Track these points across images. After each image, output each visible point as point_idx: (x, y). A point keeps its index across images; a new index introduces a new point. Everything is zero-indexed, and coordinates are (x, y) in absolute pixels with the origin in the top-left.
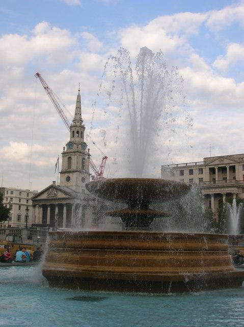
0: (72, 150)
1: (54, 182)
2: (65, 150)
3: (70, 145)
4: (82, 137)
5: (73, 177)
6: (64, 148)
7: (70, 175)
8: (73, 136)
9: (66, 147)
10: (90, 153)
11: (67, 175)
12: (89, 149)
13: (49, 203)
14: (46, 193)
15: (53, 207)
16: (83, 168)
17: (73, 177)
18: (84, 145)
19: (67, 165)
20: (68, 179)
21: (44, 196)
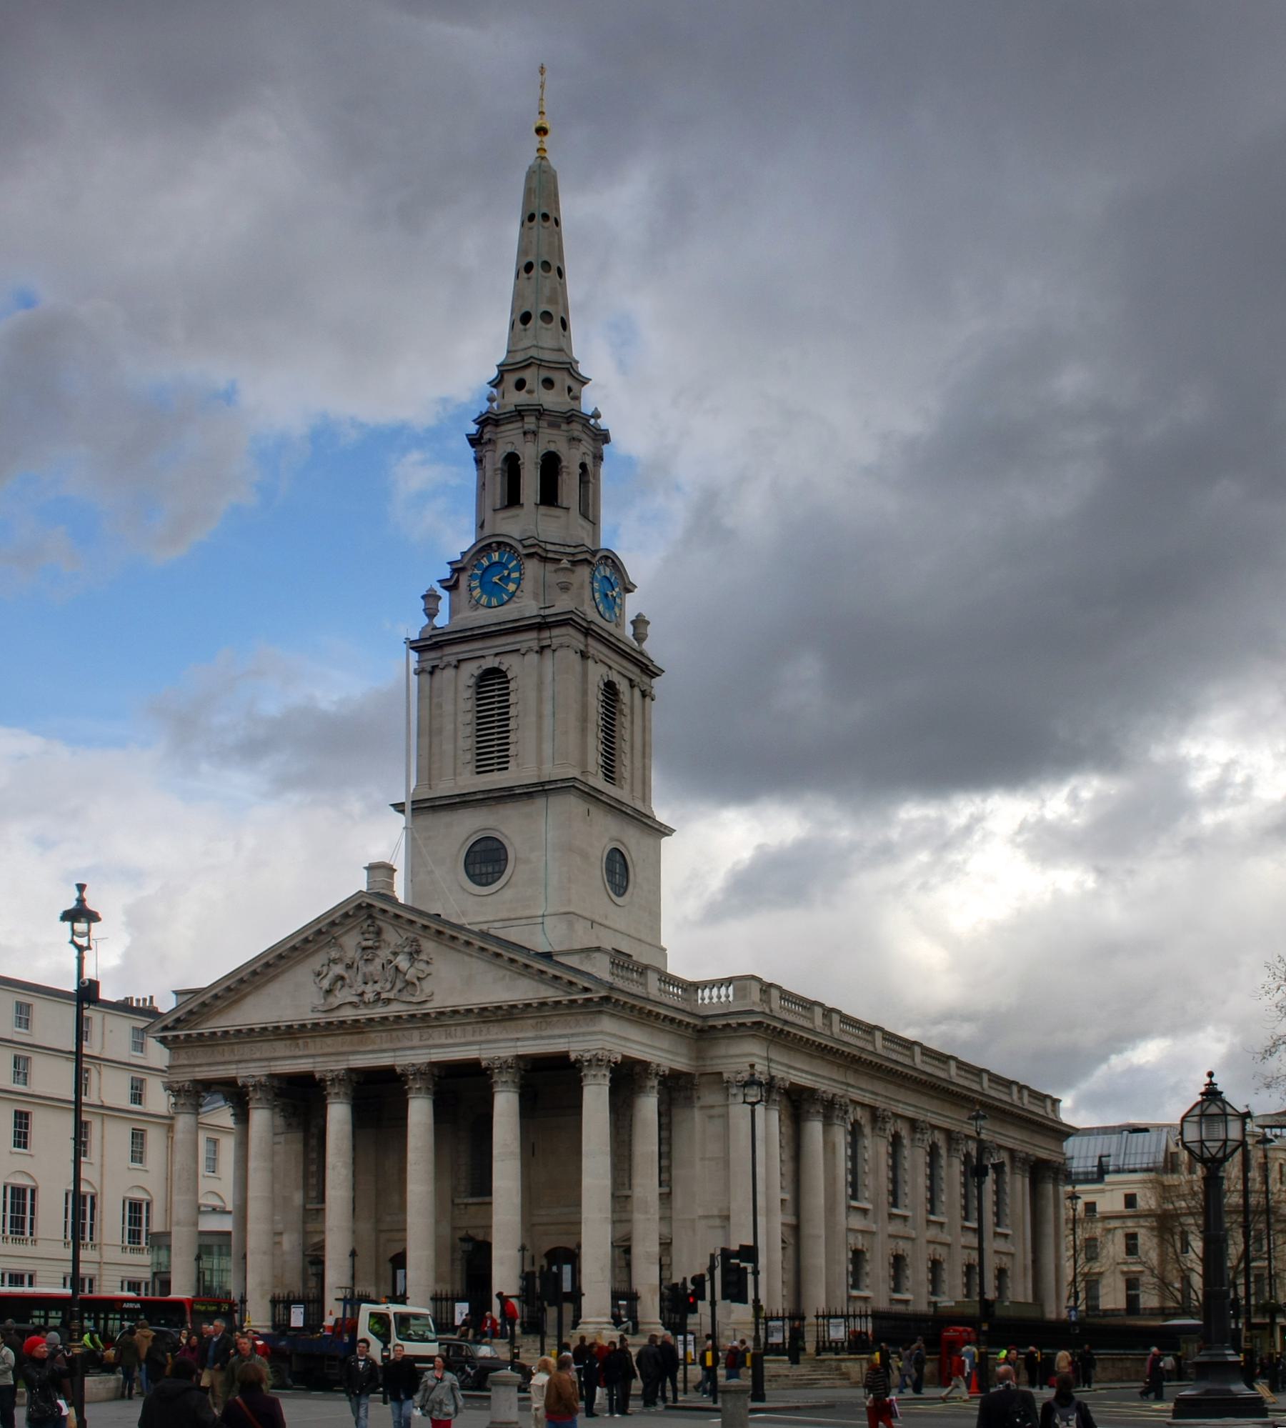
0: (509, 612)
1: (381, 870)
2: (442, 620)
3: (485, 565)
4: (588, 511)
5: (533, 835)
7: (508, 825)
9: (445, 595)
13: (340, 1065)
14: (317, 961)
15: (378, 1097)
17: (533, 835)
18: (612, 575)
19: (467, 742)
20: (486, 861)
21: (291, 1001)
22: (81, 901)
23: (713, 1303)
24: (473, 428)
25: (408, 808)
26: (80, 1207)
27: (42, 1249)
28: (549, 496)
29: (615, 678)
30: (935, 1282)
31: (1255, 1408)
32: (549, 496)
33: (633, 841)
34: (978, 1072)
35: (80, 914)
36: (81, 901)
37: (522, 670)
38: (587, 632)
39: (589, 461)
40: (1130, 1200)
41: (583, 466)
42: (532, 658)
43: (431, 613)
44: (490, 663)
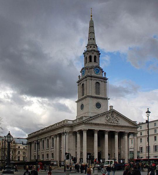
6: (79, 76)
8: (86, 63)
10: (107, 77)
11: (80, 103)
12: (105, 73)
16: (98, 92)
22: (148, 110)
23: (70, 160)
24: (100, 53)
25: (108, 99)
26: (148, 148)
27: (144, 154)
28: (91, 61)
29: (98, 81)
30: (43, 157)
31: (12, 173)
32: (91, 61)
33: (100, 101)
34: (36, 132)
35: (148, 112)
36: (148, 110)
37: (85, 83)
38: (91, 77)
39: (96, 55)
40: (24, 148)
41: (95, 57)
42: (85, 81)
43: (79, 78)
44: (82, 83)
